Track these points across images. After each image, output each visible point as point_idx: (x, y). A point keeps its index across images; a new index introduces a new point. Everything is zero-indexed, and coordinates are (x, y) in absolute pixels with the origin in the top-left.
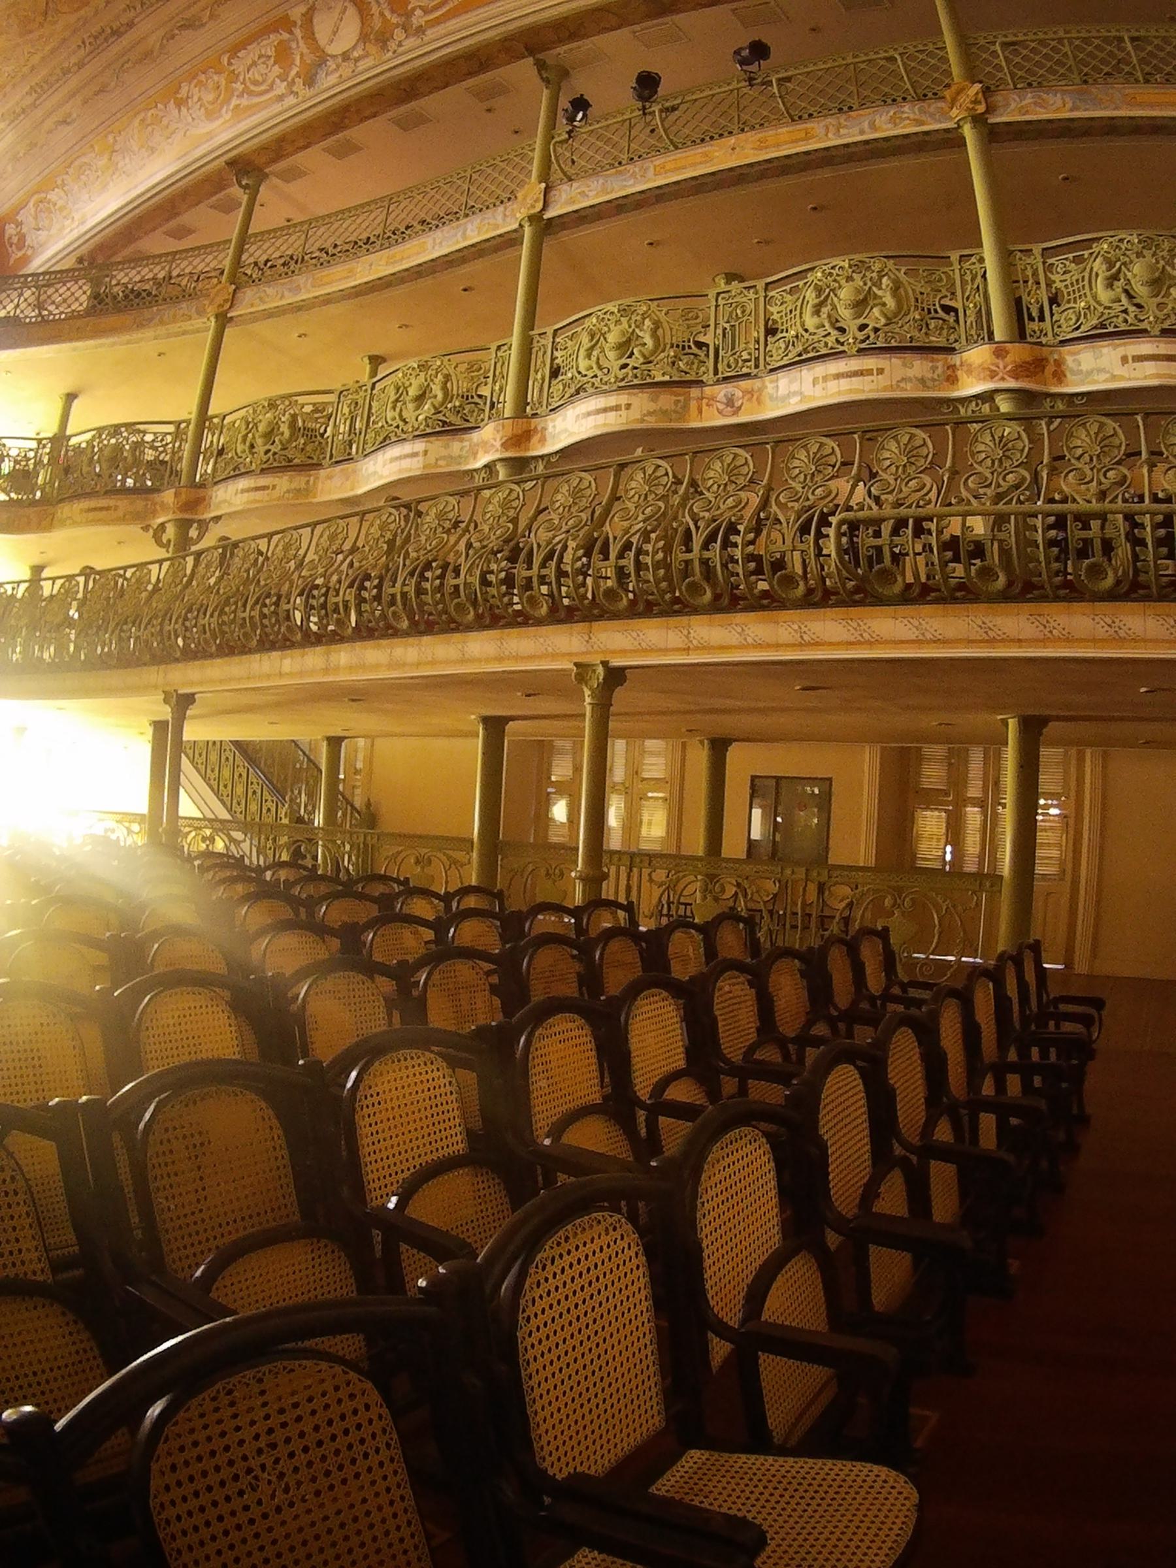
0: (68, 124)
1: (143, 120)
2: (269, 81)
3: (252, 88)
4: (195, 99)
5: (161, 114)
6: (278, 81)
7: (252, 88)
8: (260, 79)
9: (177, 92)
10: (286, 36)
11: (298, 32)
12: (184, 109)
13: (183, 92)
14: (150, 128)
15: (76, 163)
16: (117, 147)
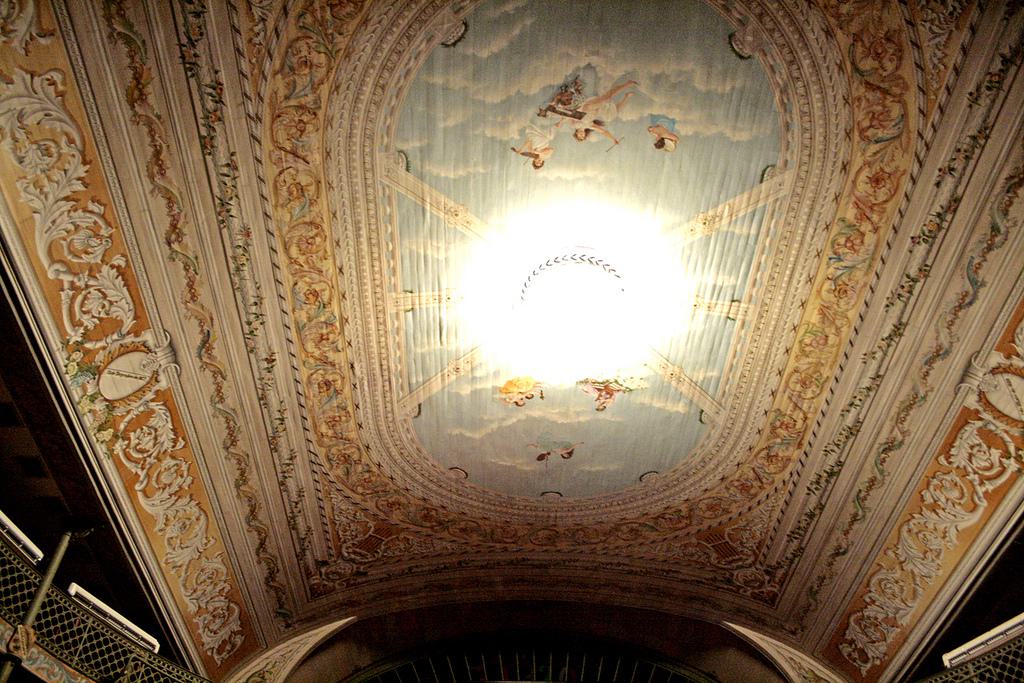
0: (844, 553)
1: (910, 531)
2: (997, 464)
3: (987, 474)
4: (943, 500)
5: (922, 522)
6: (1004, 460)
7: (987, 474)
8: (987, 465)
9: (922, 499)
10: (979, 424)
11: (987, 416)
12: (940, 512)
13: (929, 500)
14: (921, 535)
15: (874, 580)
16: (902, 559)
